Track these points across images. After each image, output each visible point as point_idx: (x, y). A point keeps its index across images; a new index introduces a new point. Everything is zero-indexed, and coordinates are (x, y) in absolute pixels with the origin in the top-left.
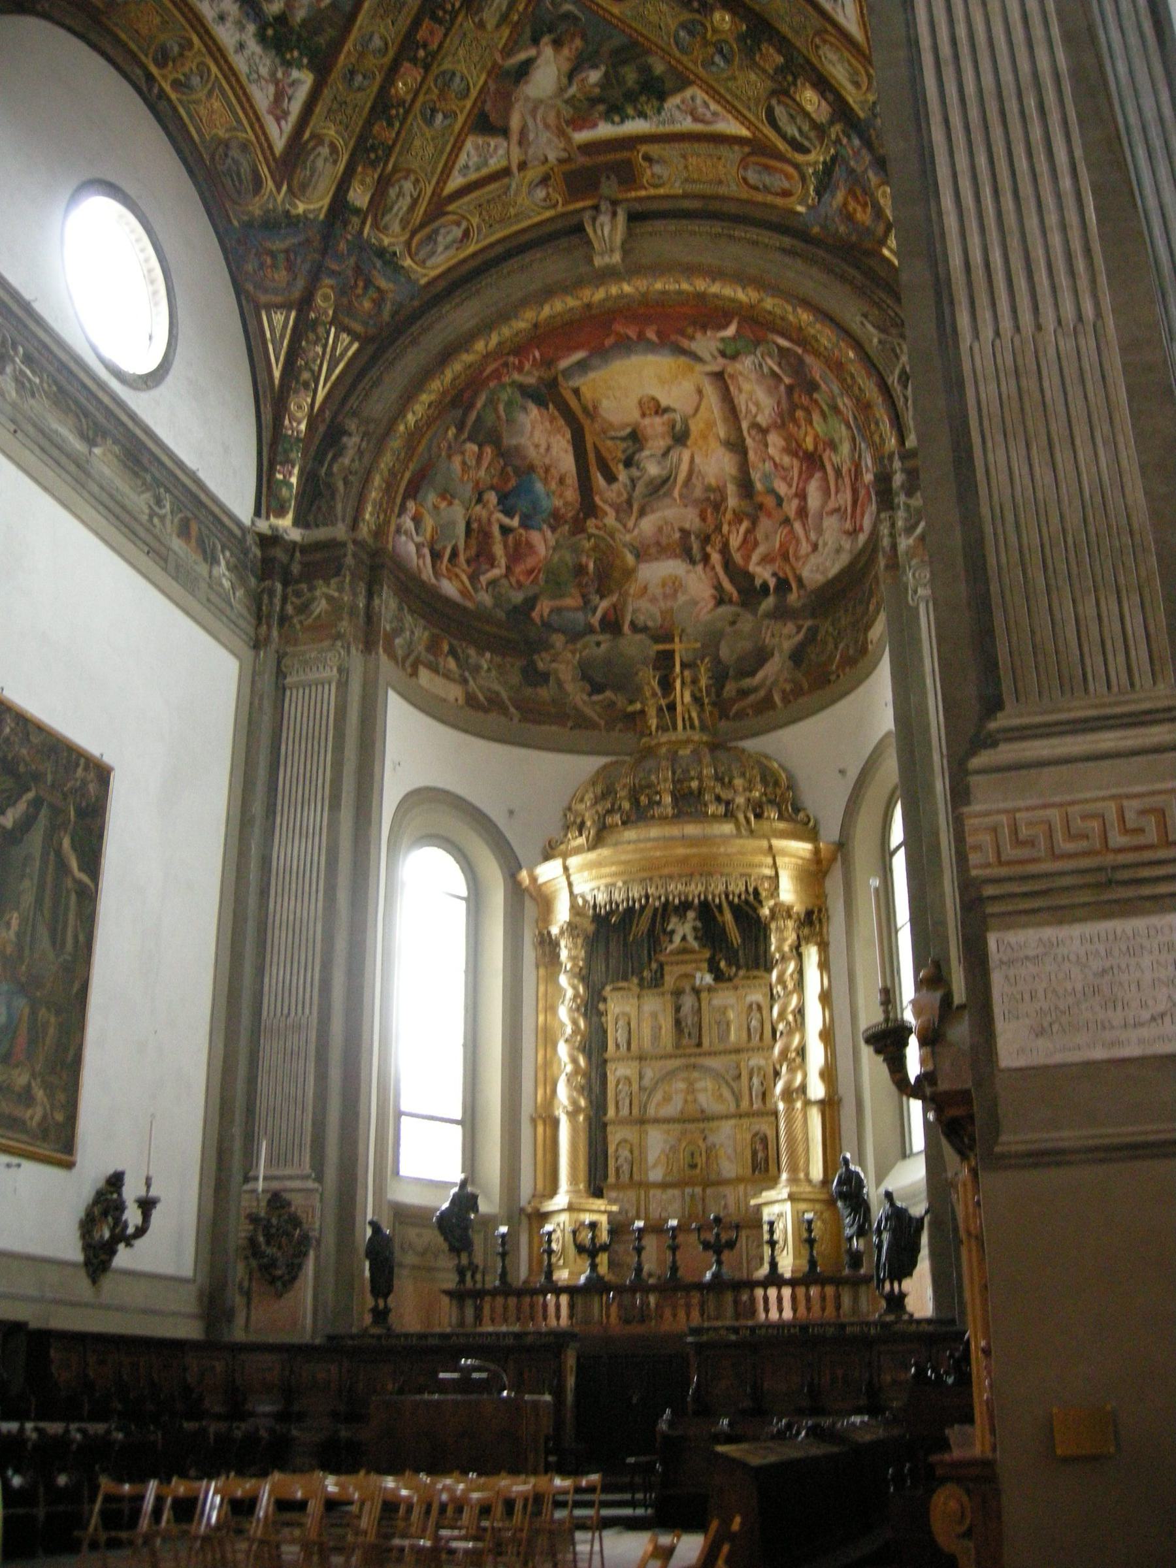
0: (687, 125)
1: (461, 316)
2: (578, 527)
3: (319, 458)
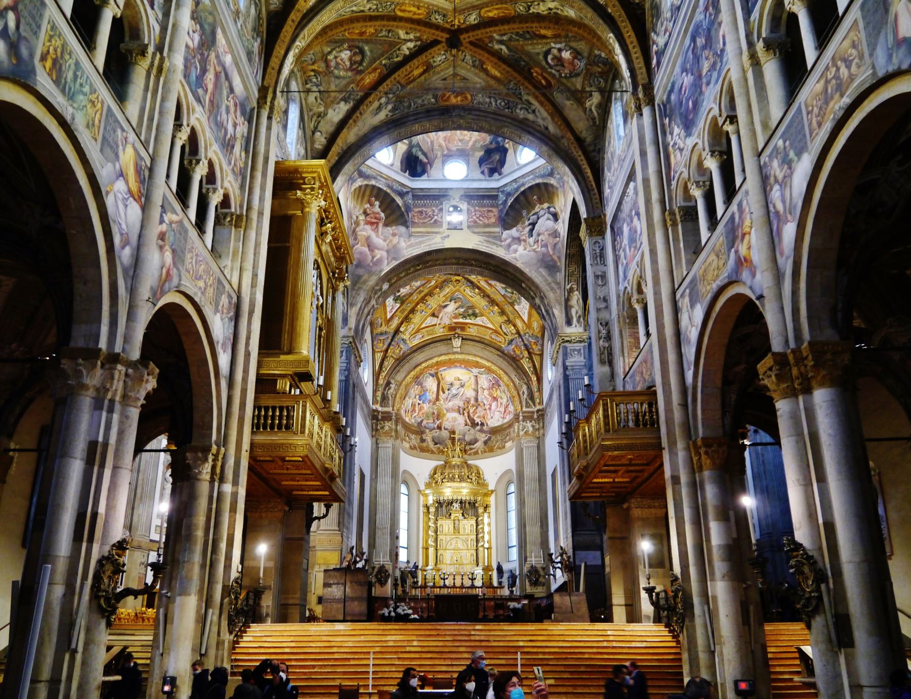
0: (481, 323)
1: (419, 357)
2: (434, 403)
3: (385, 389)
